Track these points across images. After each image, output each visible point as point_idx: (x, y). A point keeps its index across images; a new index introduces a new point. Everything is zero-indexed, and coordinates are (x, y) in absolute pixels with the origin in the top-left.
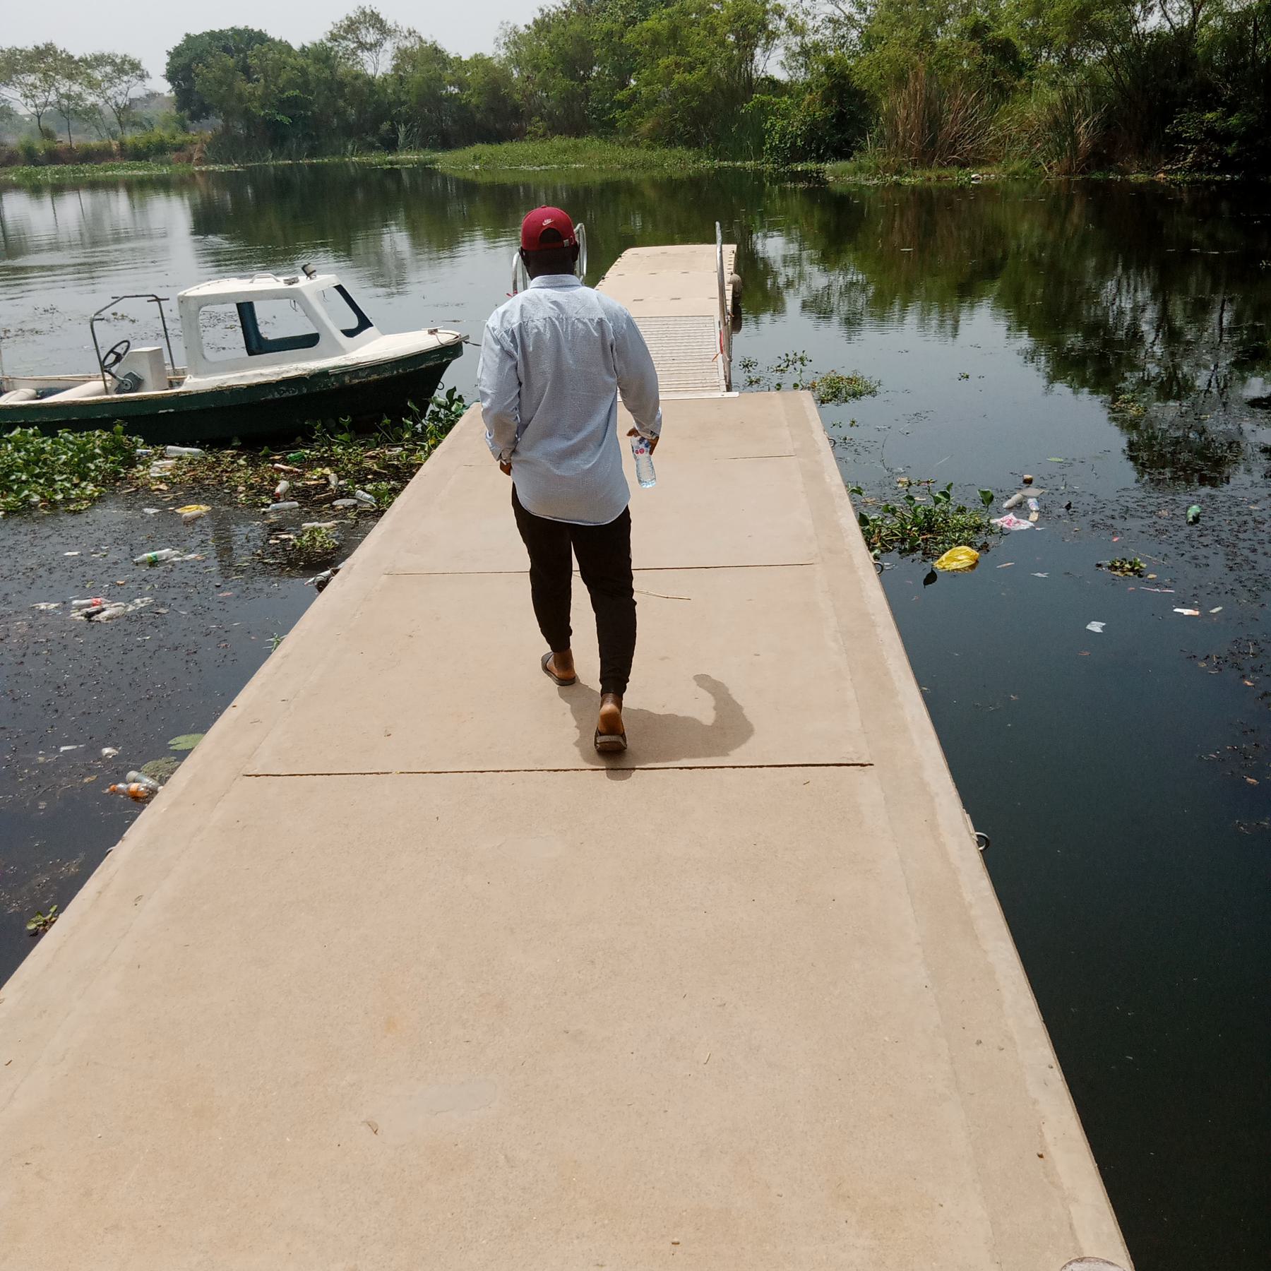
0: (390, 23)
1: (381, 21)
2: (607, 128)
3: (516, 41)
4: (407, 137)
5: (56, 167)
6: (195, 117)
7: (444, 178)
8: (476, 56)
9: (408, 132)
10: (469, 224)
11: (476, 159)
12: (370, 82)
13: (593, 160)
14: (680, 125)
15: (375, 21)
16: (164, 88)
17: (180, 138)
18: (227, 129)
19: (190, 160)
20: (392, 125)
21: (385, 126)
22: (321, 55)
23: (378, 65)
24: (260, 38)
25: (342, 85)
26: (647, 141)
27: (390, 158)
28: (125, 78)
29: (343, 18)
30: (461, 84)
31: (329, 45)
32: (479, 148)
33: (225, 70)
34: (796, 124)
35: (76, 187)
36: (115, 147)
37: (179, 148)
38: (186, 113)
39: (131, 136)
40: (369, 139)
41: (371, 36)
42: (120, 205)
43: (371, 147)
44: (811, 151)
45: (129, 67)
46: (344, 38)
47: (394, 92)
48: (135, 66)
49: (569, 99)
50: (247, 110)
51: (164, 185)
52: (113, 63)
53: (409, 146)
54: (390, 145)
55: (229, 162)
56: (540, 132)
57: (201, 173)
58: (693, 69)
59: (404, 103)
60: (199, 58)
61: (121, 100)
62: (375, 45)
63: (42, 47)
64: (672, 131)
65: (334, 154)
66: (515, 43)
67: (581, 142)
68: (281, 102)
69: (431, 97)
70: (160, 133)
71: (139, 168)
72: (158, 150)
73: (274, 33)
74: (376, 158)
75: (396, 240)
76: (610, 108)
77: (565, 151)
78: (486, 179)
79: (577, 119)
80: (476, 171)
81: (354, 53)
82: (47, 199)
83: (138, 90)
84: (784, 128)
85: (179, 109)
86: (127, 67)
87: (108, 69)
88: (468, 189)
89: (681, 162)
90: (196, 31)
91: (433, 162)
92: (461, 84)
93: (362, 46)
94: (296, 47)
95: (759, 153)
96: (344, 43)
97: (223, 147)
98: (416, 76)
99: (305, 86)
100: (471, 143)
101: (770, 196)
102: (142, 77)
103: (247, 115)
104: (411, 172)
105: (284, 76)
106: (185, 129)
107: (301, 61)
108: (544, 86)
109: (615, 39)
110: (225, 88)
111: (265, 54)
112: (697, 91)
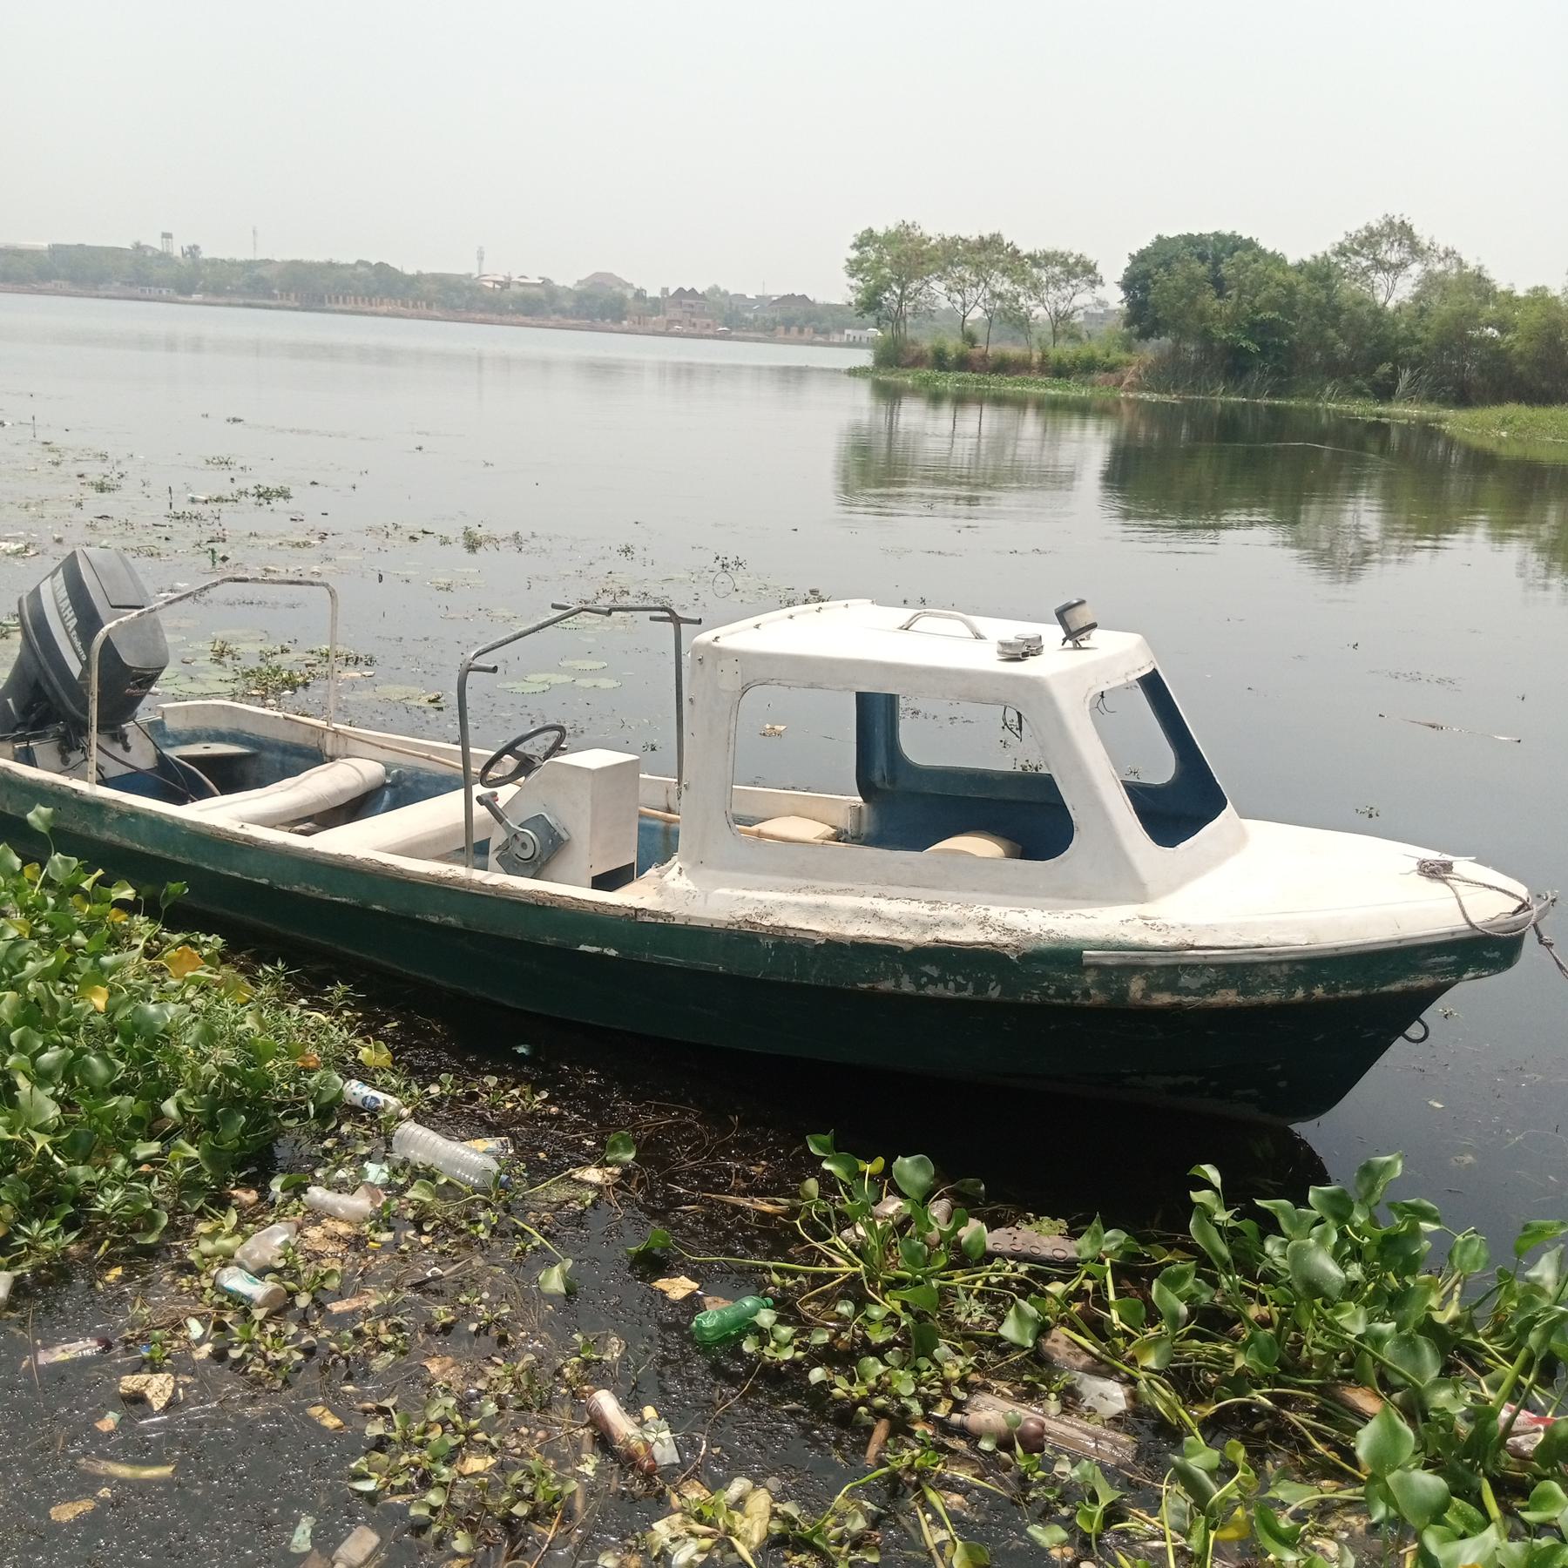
0: (1425, 243)
4: (1410, 385)
5: (961, 375)
6: (1145, 335)
7: (1450, 442)
8: (1536, 290)
10: (1473, 504)
12: (1378, 312)
15: (1402, 232)
16: (1115, 298)
17: (1118, 355)
18: (1175, 352)
19: (1119, 384)
20: (1394, 369)
21: (1385, 368)
22: (1320, 273)
23: (1395, 292)
24: (1250, 245)
25: (1338, 310)
27: (1380, 409)
28: (1074, 282)
29: (1362, 227)
31: (1334, 260)
33: (1192, 279)
36: (1035, 360)
37: (1110, 369)
38: (1136, 329)
39: (1065, 350)
40: (1358, 382)
43: (1358, 393)
45: (1083, 270)
46: (1357, 253)
47: (1408, 327)
48: (1089, 269)
51: (1083, 409)
52: (1065, 263)
53: (1410, 397)
54: (1385, 392)
55: (1167, 391)
57: (1129, 401)
59: (1419, 341)
60: (1166, 264)
65: (1304, 396)
68: (1253, 324)
69: (1455, 338)
72: (1088, 367)
73: (1268, 244)
74: (1363, 409)
75: (1364, 514)
78: (1515, 451)
82: (946, 410)
85: (1128, 324)
87: (1057, 270)
88: (1481, 462)
91: (1439, 421)
93: (1380, 265)
94: (1292, 260)
96: (1355, 259)
97: (1166, 374)
98: (1443, 310)
99: (1288, 308)
100: (1498, 399)
102: (1093, 283)
103: (1206, 336)
104: (1405, 430)
105: (1264, 295)
106: (1129, 349)
107: (1292, 277)
111: (1247, 264)
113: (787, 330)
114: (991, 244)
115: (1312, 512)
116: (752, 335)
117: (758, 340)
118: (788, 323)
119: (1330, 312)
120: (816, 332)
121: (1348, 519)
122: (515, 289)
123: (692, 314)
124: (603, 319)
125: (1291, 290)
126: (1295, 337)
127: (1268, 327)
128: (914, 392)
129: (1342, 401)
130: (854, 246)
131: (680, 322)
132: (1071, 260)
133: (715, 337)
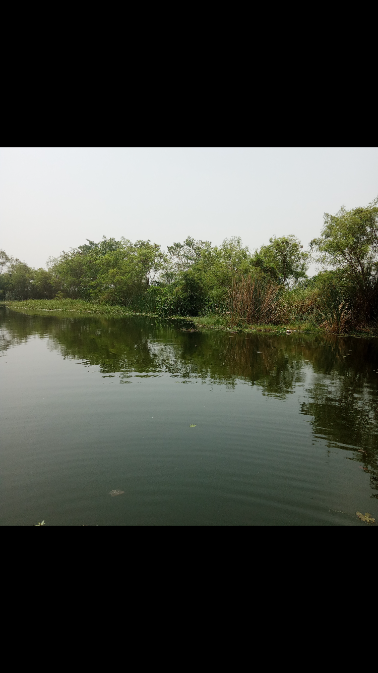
0: (10, 257)
11: (26, 305)
32: (31, 302)
34: (171, 299)
53: (10, 299)
67: (74, 301)
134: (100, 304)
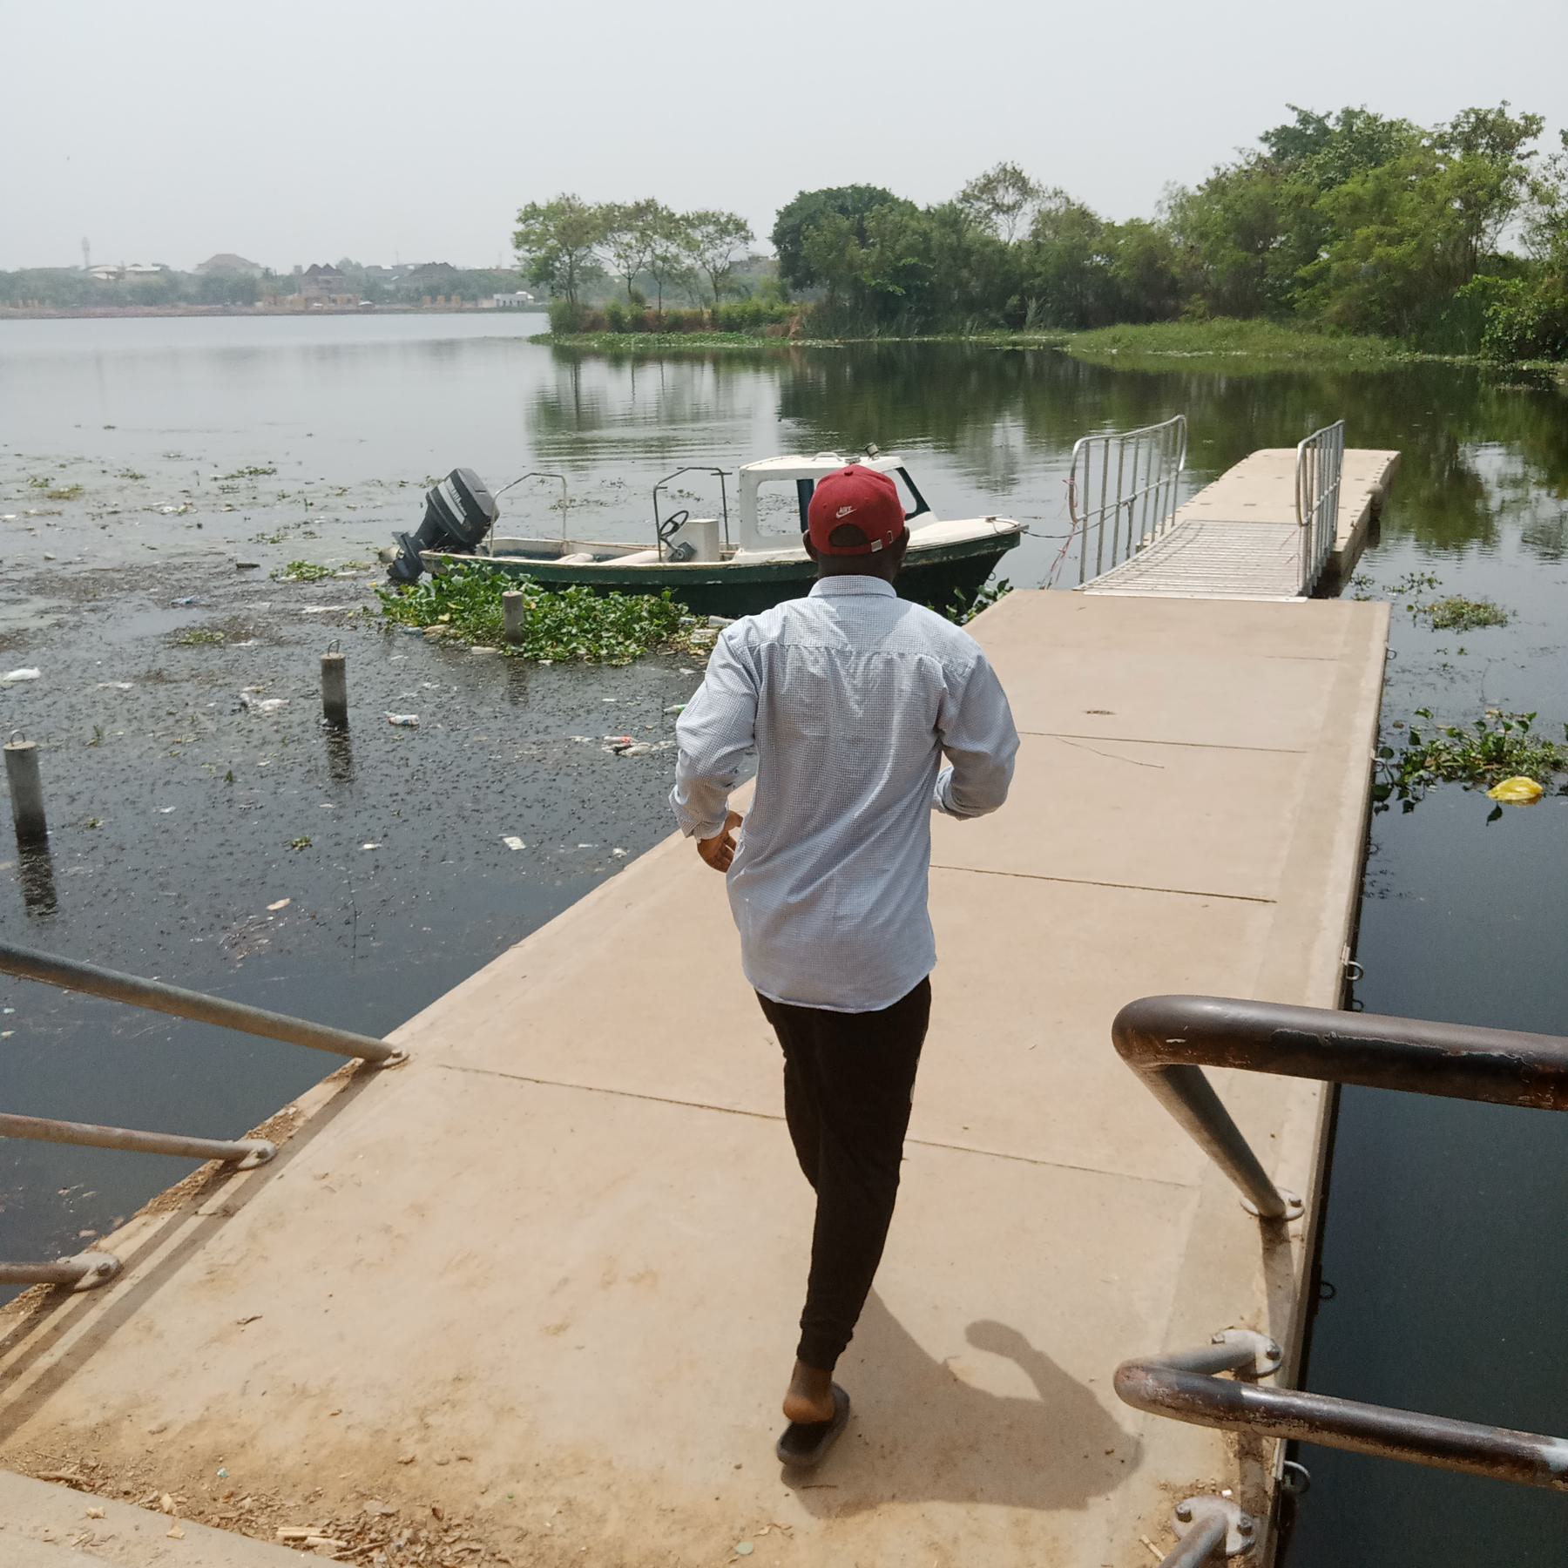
0: (1032, 183)
1: (1024, 181)
2: (1282, 310)
3: (1184, 204)
4: (1037, 314)
5: (641, 335)
6: (798, 285)
7: (1077, 364)
9: (1040, 307)
10: (1098, 417)
12: (1002, 249)
13: (1259, 346)
14: (1376, 309)
16: (769, 251)
17: (779, 307)
18: (832, 300)
19: (786, 333)
20: (1022, 300)
21: (1014, 300)
22: (949, 218)
23: (1014, 230)
24: (883, 197)
25: (968, 252)
26: (1332, 327)
27: (1014, 337)
28: (728, 239)
29: (980, 174)
30: (1110, 254)
31: (960, 206)
32: (1124, 330)
33: (838, 233)
35: (659, 359)
36: (706, 316)
37: (777, 320)
38: (789, 280)
39: (726, 304)
40: (992, 315)
41: (1009, 197)
42: (704, 379)
43: (994, 325)
44: (1545, 346)
45: (735, 228)
46: (978, 199)
47: (1029, 261)
48: (740, 226)
49: (1242, 273)
50: (856, 279)
51: (755, 360)
52: (717, 222)
53: (1039, 325)
54: (1017, 322)
55: (829, 337)
56: (1200, 311)
57: (796, 348)
58: (1400, 241)
59: (1040, 274)
60: (812, 218)
61: (720, 263)
62: (1014, 207)
63: (643, 203)
64: (1365, 316)
65: (948, 331)
66: (1181, 206)
68: (897, 270)
69: (1072, 268)
70: (759, 302)
71: (730, 341)
72: (754, 321)
73: (900, 193)
74: (999, 339)
75: (1010, 433)
76: (1292, 285)
77: (1226, 335)
78: (1123, 366)
79: (1246, 299)
80: (1113, 357)
81: (987, 215)
82: (627, 369)
83: (739, 253)
84: (1510, 317)
85: (783, 275)
86: (730, 227)
87: (711, 229)
88: (1103, 377)
89: (1374, 353)
90: (811, 189)
91: (1063, 344)
92: (1110, 254)
93: (998, 208)
94: (922, 207)
95: (1475, 347)
96: (977, 205)
97: (824, 322)
98: (1056, 242)
99: (925, 254)
100: (1111, 322)
101: (1484, 399)
102: (746, 239)
103: (857, 286)
104: (1037, 354)
105: (903, 242)
106: (786, 298)
107: (925, 225)
108: (1211, 256)
109: (1305, 204)
110: (834, 254)
111: (884, 216)
112: (1402, 268)
113: (434, 299)
114: (645, 210)
115: (967, 436)
116: (398, 306)
117: (405, 312)
118: (433, 292)
119: (962, 254)
120: (463, 298)
121: (997, 439)
122: (129, 278)
123: (330, 290)
124: (233, 303)
125: (926, 236)
126: (934, 278)
127: (911, 271)
128: (597, 354)
129: (980, 334)
130: (520, 220)
131: (317, 299)
132: (723, 219)
133: (358, 312)
134: (1320, 332)
